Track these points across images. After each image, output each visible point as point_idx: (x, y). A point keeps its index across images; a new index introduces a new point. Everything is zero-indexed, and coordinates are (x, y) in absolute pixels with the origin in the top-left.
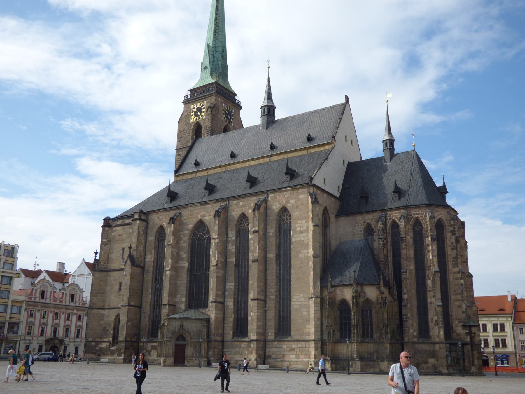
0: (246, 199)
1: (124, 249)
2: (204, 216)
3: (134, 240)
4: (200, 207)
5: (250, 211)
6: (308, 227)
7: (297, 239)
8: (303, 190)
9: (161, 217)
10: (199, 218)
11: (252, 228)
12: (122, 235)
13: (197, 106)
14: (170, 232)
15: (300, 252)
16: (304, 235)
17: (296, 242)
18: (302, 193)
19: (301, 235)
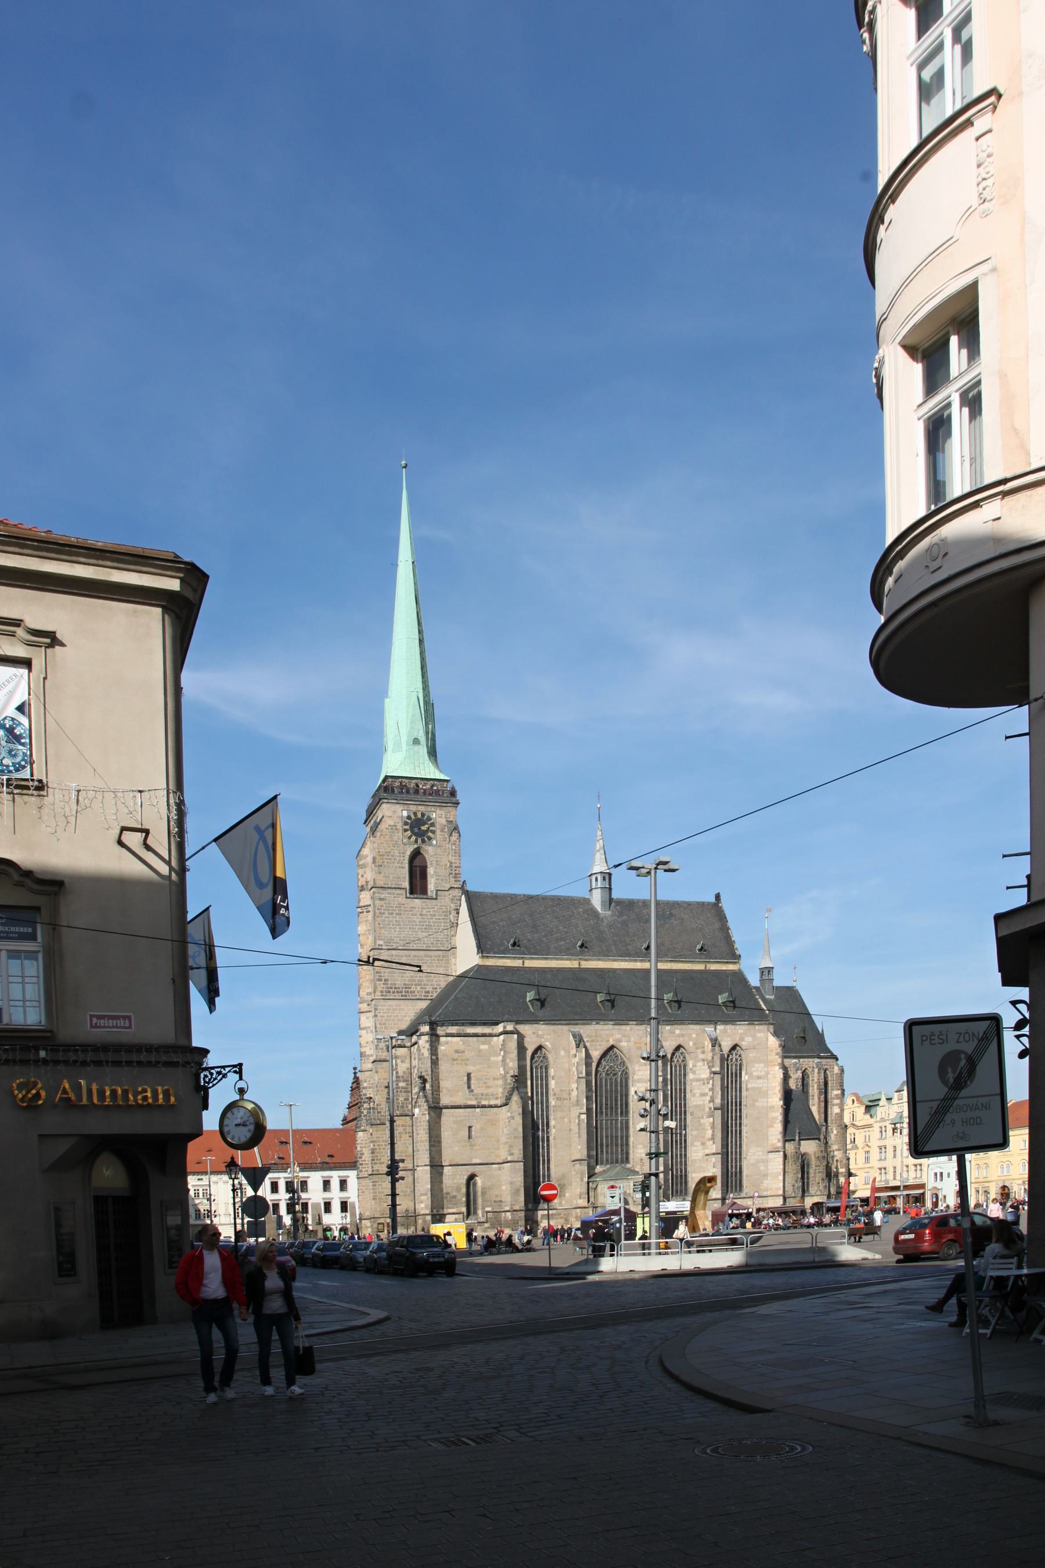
0: (683, 1027)
1: (469, 1075)
2: (621, 1041)
3: (511, 1064)
4: (611, 1027)
5: (691, 1044)
6: (768, 1073)
7: (754, 1085)
8: (761, 1027)
9: (540, 1033)
10: (611, 1043)
11: (695, 1066)
12: (463, 1052)
13: (415, 814)
14: (580, 1059)
15: (757, 1101)
16: (761, 1081)
17: (753, 1088)
18: (760, 1031)
19: (759, 1081)
